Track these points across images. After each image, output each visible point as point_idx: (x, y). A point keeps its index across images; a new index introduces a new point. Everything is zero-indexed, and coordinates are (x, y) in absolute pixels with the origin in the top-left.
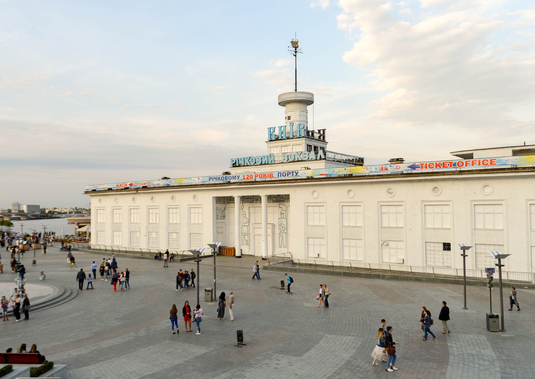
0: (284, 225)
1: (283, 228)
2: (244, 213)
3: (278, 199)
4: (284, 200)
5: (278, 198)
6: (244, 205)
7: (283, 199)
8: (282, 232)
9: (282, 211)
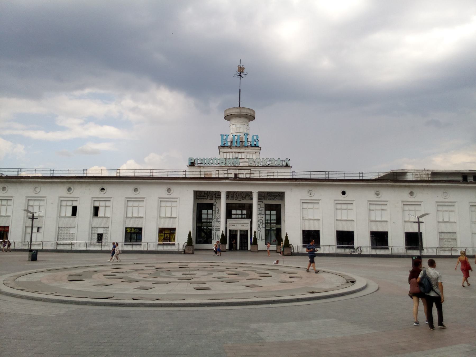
0: (262, 220)
1: (262, 223)
2: (217, 209)
4: (263, 198)
6: (216, 201)
7: (262, 197)
8: (261, 226)
9: (260, 208)
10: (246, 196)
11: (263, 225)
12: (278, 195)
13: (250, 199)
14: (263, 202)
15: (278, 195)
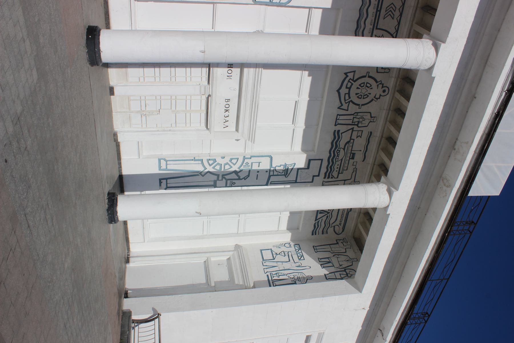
3: (342, 150)
5: (345, 154)
7: (335, 174)
10: (352, 117)
11: (227, 180)
12: (332, 221)
13: (339, 131)
14: (318, 176)
15: (332, 221)
